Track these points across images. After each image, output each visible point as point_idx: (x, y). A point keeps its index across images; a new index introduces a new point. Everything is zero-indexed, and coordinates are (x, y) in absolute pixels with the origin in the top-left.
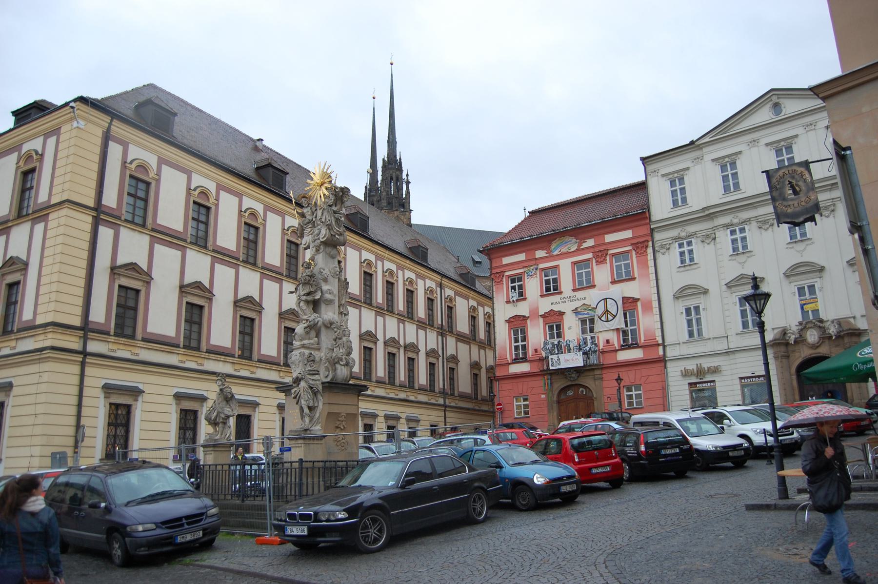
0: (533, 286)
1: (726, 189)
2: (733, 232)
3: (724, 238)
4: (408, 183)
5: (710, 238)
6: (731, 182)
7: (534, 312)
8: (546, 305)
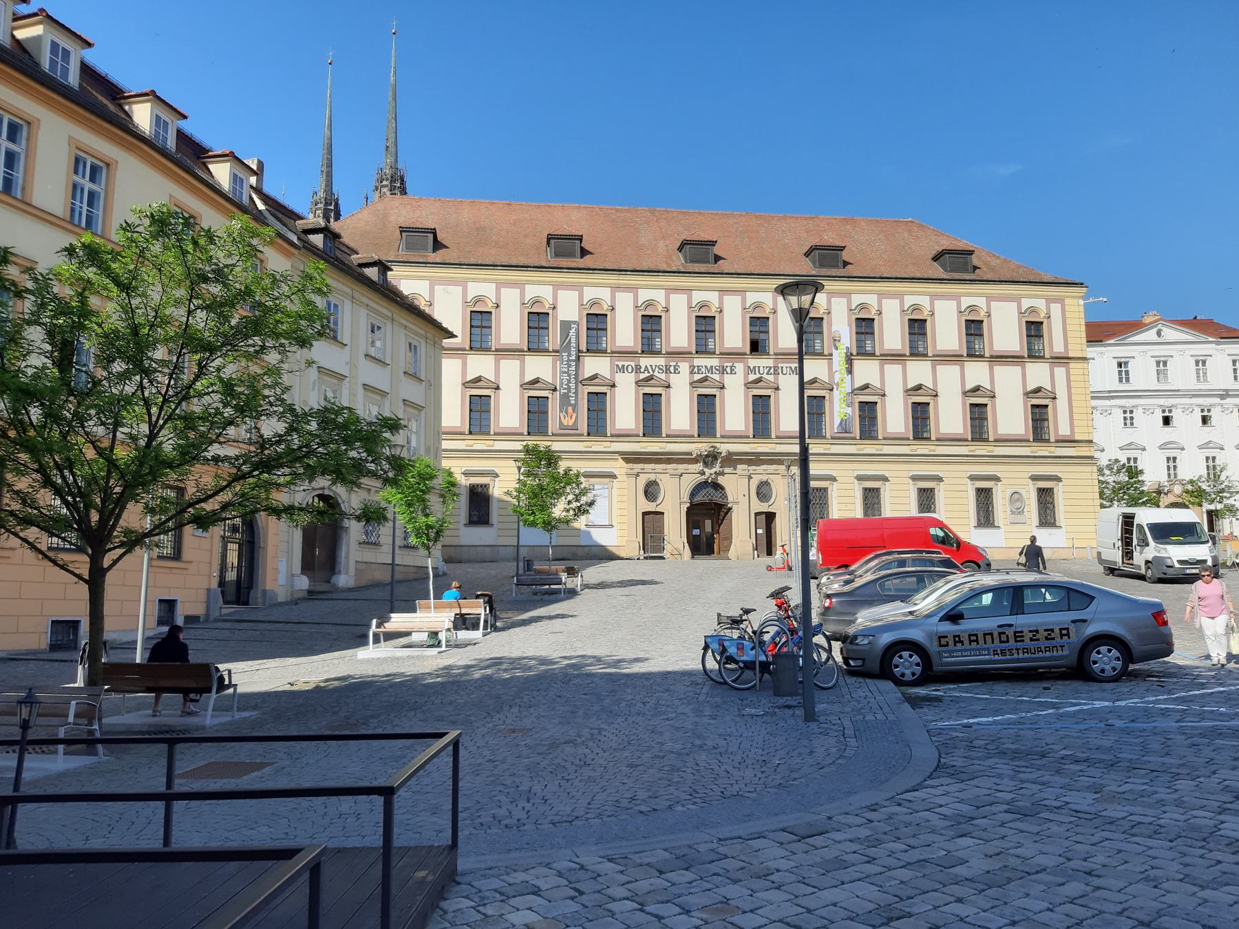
2: (1125, 412)
5: (1106, 412)
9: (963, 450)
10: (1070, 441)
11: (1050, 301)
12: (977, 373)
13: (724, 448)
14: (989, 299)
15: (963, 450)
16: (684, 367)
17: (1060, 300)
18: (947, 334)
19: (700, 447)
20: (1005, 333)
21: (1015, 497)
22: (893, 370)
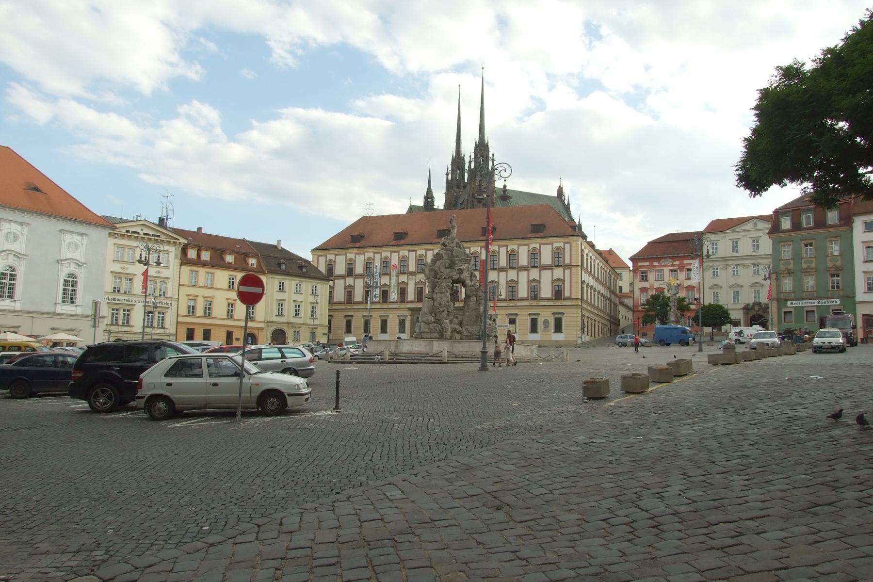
0: (651, 276)
1: (733, 251)
3: (730, 269)
4: (493, 161)
6: (735, 249)
9: (527, 304)
10: (569, 299)
11: (565, 243)
12: (534, 274)
14: (541, 244)
15: (527, 304)
17: (570, 243)
18: (523, 260)
21: (546, 322)
22: (503, 275)
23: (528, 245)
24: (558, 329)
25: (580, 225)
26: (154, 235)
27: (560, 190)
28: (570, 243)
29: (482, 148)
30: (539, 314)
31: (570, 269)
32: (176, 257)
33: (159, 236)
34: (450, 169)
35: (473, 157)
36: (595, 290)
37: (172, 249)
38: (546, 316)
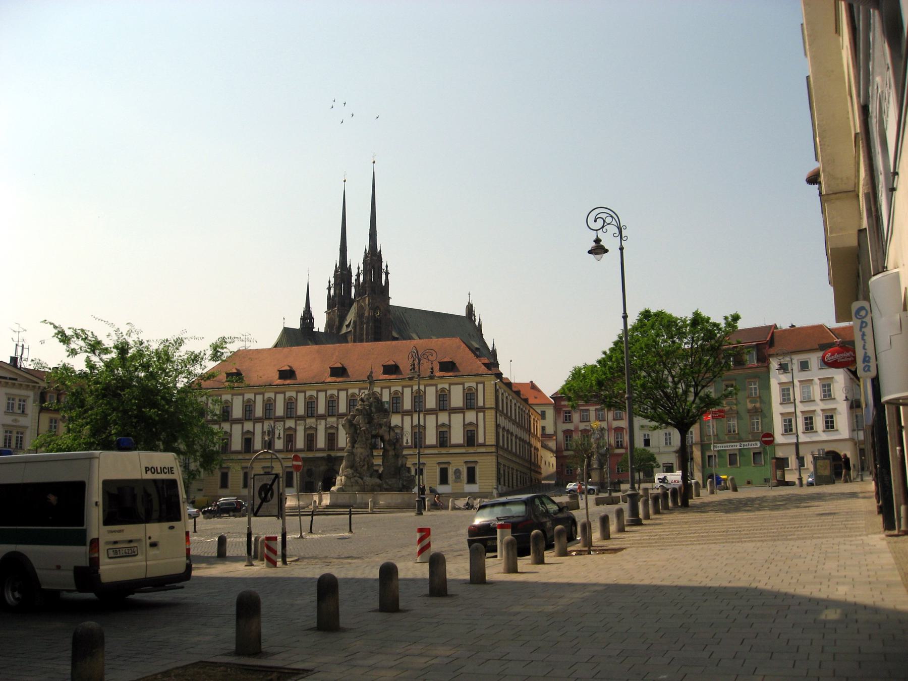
0: (576, 417)
4: (387, 274)
7: (577, 429)
8: (582, 426)
10: (483, 445)
12: (443, 418)
13: (333, 454)
14: (450, 385)
16: (323, 422)
17: (483, 383)
18: (431, 402)
19: (324, 454)
20: (457, 399)
21: (457, 472)
22: (407, 419)
23: (436, 385)
24: (471, 479)
25: (494, 351)
26: (10, 379)
27: (470, 308)
28: (483, 383)
29: (373, 258)
30: (449, 463)
31: (484, 412)
32: (34, 401)
33: (16, 379)
34: (332, 282)
35: (362, 268)
36: (512, 434)
37: (31, 394)
38: (458, 464)
